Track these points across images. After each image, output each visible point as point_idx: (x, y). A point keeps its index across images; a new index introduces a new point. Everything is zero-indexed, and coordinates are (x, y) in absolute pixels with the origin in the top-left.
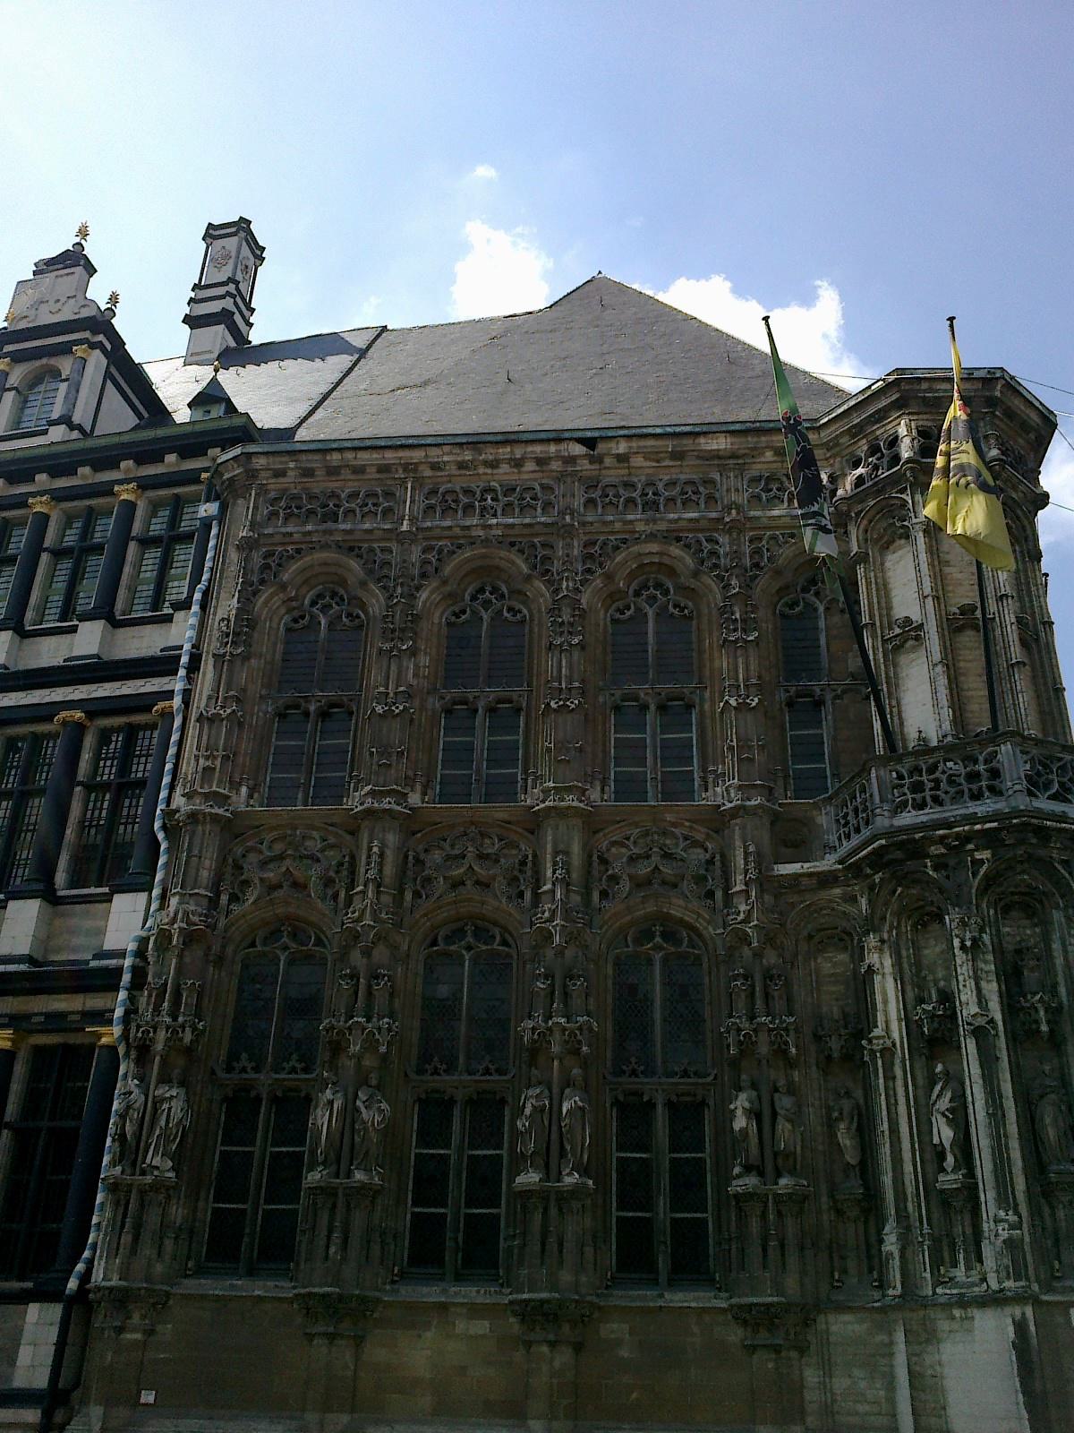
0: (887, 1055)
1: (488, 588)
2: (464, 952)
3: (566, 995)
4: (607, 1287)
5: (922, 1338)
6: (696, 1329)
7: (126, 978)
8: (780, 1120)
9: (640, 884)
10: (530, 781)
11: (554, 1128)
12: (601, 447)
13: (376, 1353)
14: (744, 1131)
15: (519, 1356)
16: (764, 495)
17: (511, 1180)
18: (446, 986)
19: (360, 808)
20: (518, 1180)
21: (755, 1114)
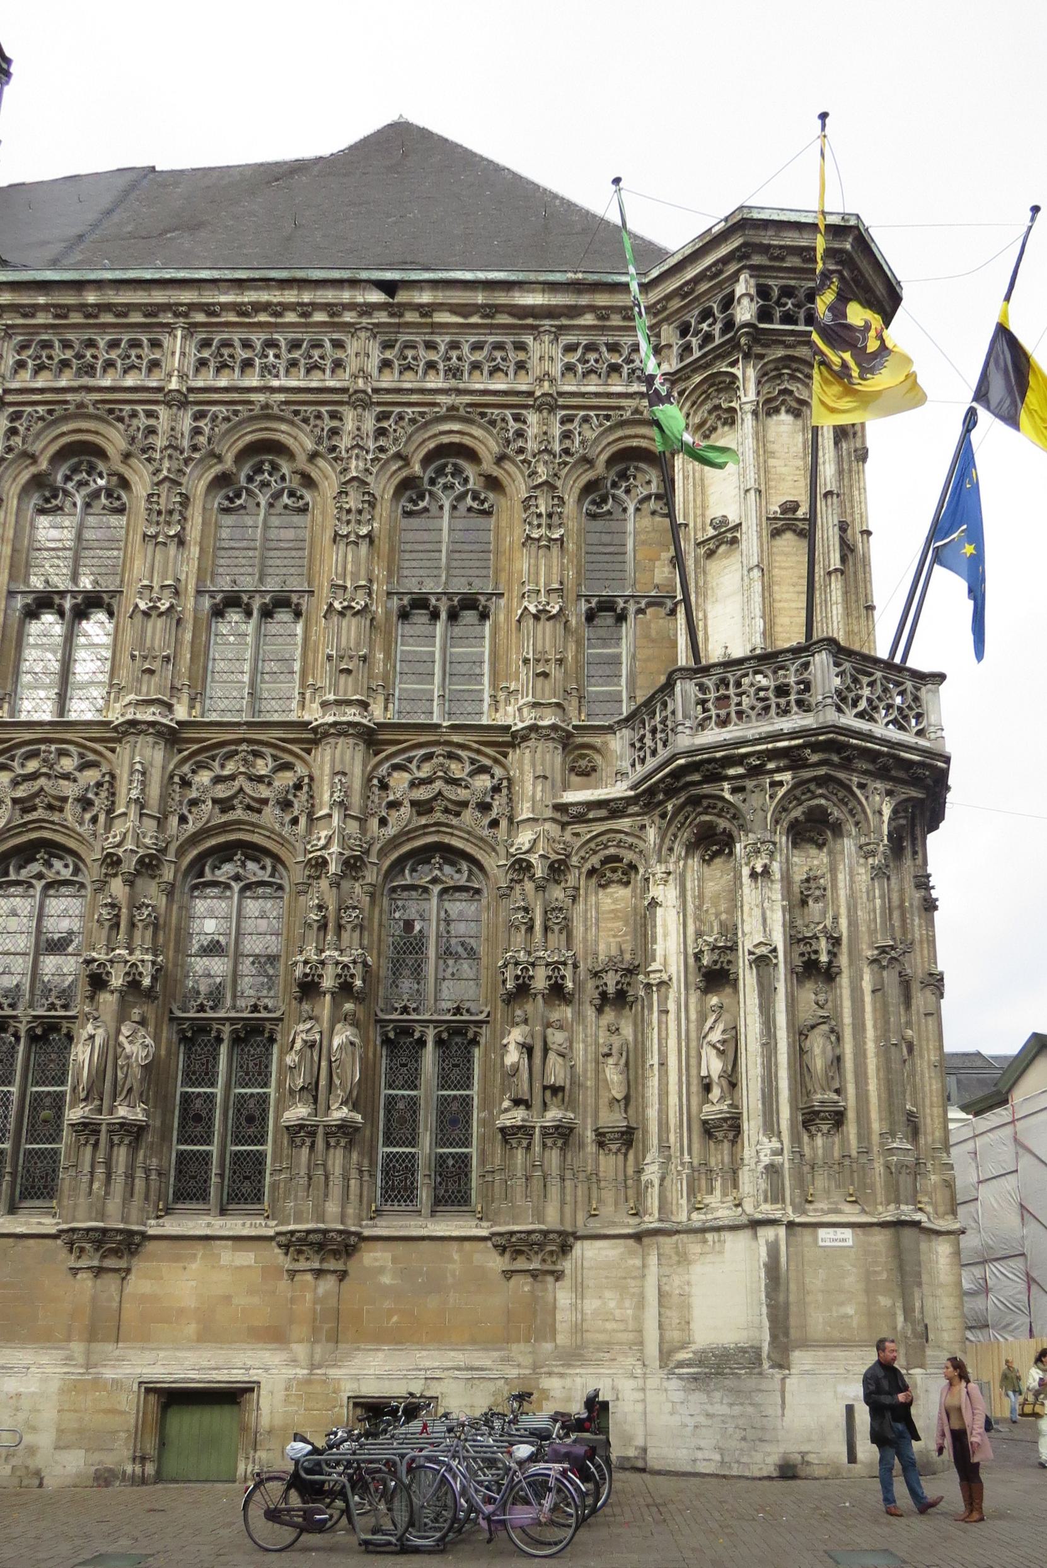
0: (663, 989)
1: (267, 467)
2: (233, 884)
3: (340, 927)
4: (372, 1219)
8: (552, 1056)
9: (422, 807)
10: (308, 696)
11: (324, 1064)
13: (139, 1284)
14: (516, 1069)
15: (283, 1284)
16: (580, 366)
17: (278, 1117)
18: (214, 921)
19: (121, 720)
20: (287, 1115)
21: (528, 1049)
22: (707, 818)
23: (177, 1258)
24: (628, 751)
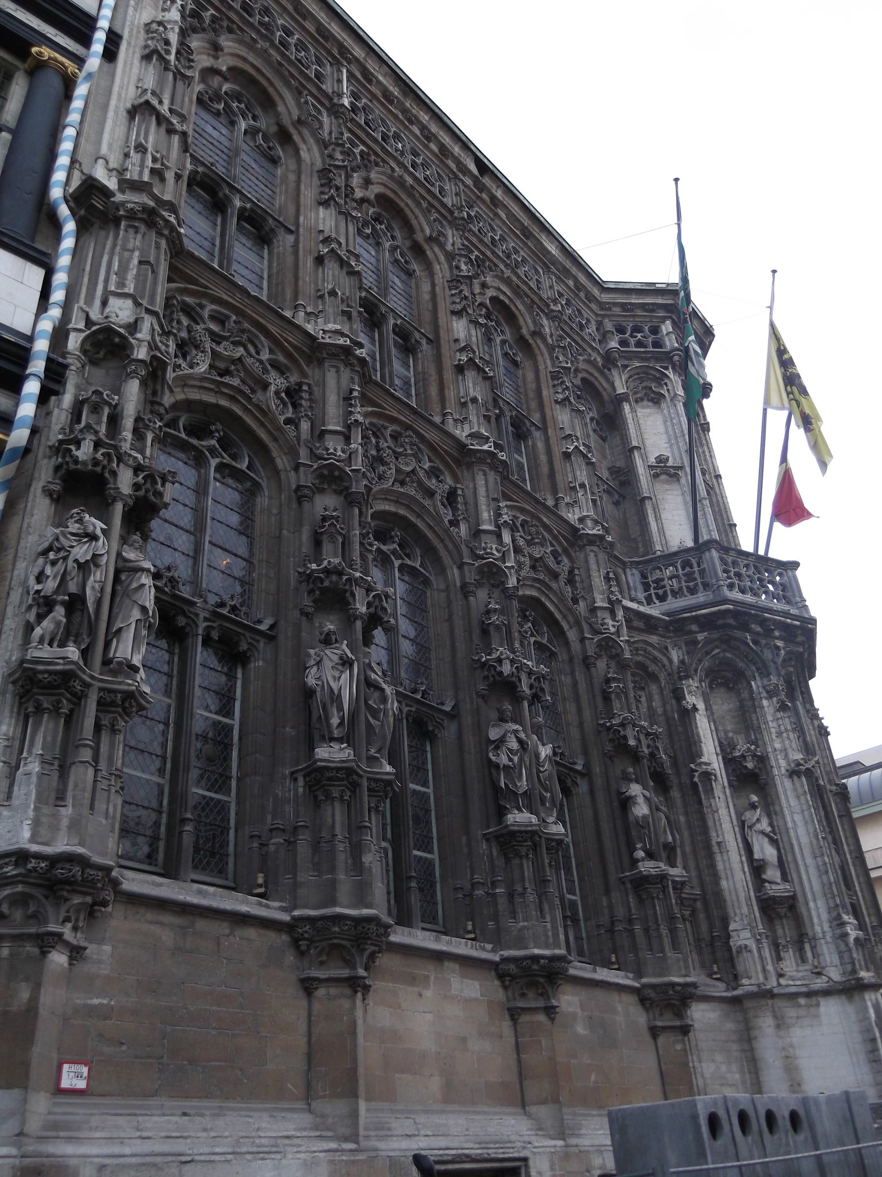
5: (781, 1024)
6: (620, 1008)
7: (38, 366)
12: (486, 181)
22: (728, 655)
23: (413, 980)
24: (640, 588)
